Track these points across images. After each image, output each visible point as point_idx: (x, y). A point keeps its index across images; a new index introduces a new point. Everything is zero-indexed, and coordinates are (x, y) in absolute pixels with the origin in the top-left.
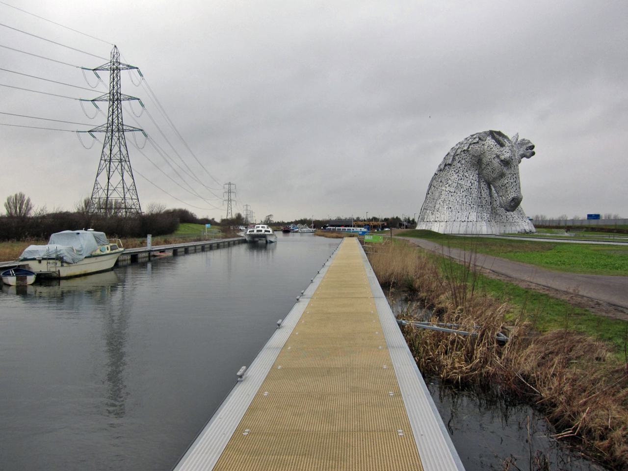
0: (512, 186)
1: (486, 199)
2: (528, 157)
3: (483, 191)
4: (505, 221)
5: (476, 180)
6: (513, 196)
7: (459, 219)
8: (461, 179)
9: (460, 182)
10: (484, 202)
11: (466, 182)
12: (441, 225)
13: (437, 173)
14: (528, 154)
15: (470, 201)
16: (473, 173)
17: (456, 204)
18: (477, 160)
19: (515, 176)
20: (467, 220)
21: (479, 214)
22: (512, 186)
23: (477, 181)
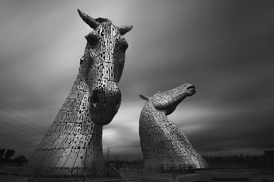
0: (98, 71)
2: (190, 95)
4: (172, 156)
15: (68, 118)
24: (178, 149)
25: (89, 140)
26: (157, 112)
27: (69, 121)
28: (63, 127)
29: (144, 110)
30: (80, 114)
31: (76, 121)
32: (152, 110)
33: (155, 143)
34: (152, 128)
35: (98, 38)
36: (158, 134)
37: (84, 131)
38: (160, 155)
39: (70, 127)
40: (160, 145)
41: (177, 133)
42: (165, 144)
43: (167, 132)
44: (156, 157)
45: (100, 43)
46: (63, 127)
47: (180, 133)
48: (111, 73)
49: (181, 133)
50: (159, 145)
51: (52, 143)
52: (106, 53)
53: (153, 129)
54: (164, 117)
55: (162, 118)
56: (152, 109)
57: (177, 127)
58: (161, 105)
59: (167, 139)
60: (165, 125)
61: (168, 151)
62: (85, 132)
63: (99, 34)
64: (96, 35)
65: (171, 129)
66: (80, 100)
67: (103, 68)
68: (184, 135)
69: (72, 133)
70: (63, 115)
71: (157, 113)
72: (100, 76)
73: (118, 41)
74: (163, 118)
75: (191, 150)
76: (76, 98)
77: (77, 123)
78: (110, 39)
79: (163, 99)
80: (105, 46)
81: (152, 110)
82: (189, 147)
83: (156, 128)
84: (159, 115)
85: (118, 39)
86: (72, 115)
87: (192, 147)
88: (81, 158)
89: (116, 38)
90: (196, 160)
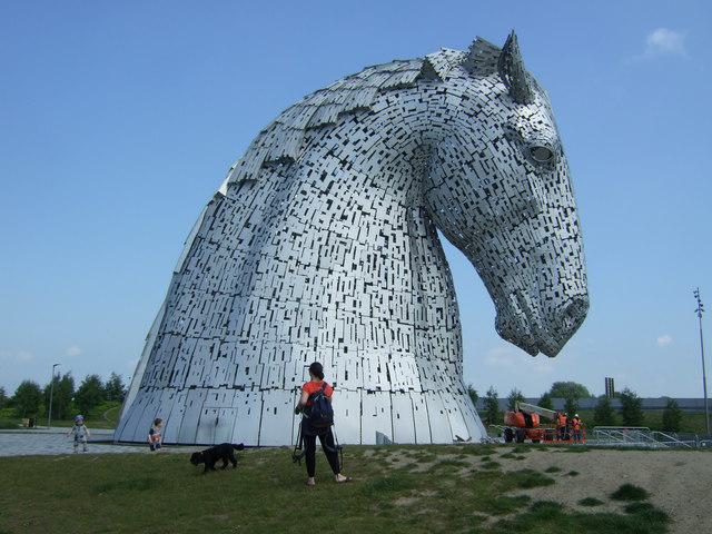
6: (571, 293)
7: (353, 383)
8: (344, 217)
9: (338, 227)
10: (432, 314)
11: (364, 228)
15: (385, 307)
17: (331, 314)
18: (409, 150)
22: (567, 251)
23: (405, 230)
27: (394, 317)
28: (380, 332)
31: (417, 323)
37: (443, 351)
51: (383, 375)
86: (395, 301)
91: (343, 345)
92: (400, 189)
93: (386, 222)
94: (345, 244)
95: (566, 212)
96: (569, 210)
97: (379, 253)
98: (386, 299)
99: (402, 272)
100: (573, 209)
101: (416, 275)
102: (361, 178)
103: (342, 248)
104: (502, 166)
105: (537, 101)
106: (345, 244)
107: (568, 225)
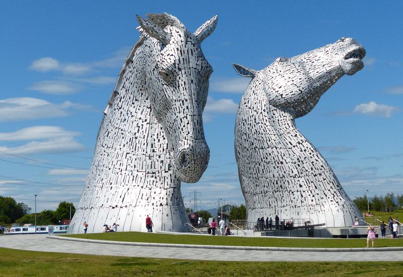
1: (162, 158)
2: (352, 72)
3: (157, 140)
5: (146, 120)
6: (181, 148)
7: (109, 203)
10: (158, 164)
12: (84, 216)
13: (106, 112)
14: (348, 67)
15: (132, 165)
16: (142, 105)
19: (186, 104)
20: (119, 205)
21: (146, 191)
24: (309, 192)
25: (171, 195)
26: (275, 112)
27: (136, 169)
29: (245, 103)
30: (150, 161)
32: (263, 109)
33: (268, 180)
34: (262, 148)
35: (175, 74)
36: (275, 162)
38: (276, 202)
39: (140, 178)
40: (277, 183)
41: (313, 160)
42: (286, 183)
43: (293, 158)
44: (270, 205)
45: (178, 81)
46: (128, 177)
47: (317, 161)
48: (197, 129)
49: (319, 160)
50: (275, 183)
52: (188, 100)
53: (265, 150)
54: (288, 124)
55: (284, 126)
56: (263, 106)
57: (312, 149)
58: (282, 98)
59: (291, 173)
60: (290, 142)
61: (291, 195)
62: (163, 185)
63: (175, 67)
64: (172, 70)
65: (301, 151)
66: (144, 138)
67: (188, 123)
68: (324, 166)
69: (145, 186)
70: (119, 158)
71: (274, 114)
72: (186, 133)
73: (201, 73)
74: (286, 127)
75: (335, 194)
76: (135, 133)
77: (148, 173)
78: (190, 75)
79: (288, 84)
80: (186, 89)
81: (263, 109)
82: (331, 187)
83: (270, 150)
84: (278, 120)
85: (200, 70)
87: (338, 188)
88: (167, 215)
89: (197, 71)
90: (340, 210)
91: (111, 186)
92: (147, 99)
93: (140, 119)
94: (122, 134)
95: (183, 101)
96: (185, 101)
97: (134, 136)
98: (134, 159)
99: (142, 144)
100: (186, 101)
101: (150, 145)
102: (132, 96)
103: (122, 136)
104: (156, 84)
105: (171, 42)
106: (122, 134)
107: (184, 110)
